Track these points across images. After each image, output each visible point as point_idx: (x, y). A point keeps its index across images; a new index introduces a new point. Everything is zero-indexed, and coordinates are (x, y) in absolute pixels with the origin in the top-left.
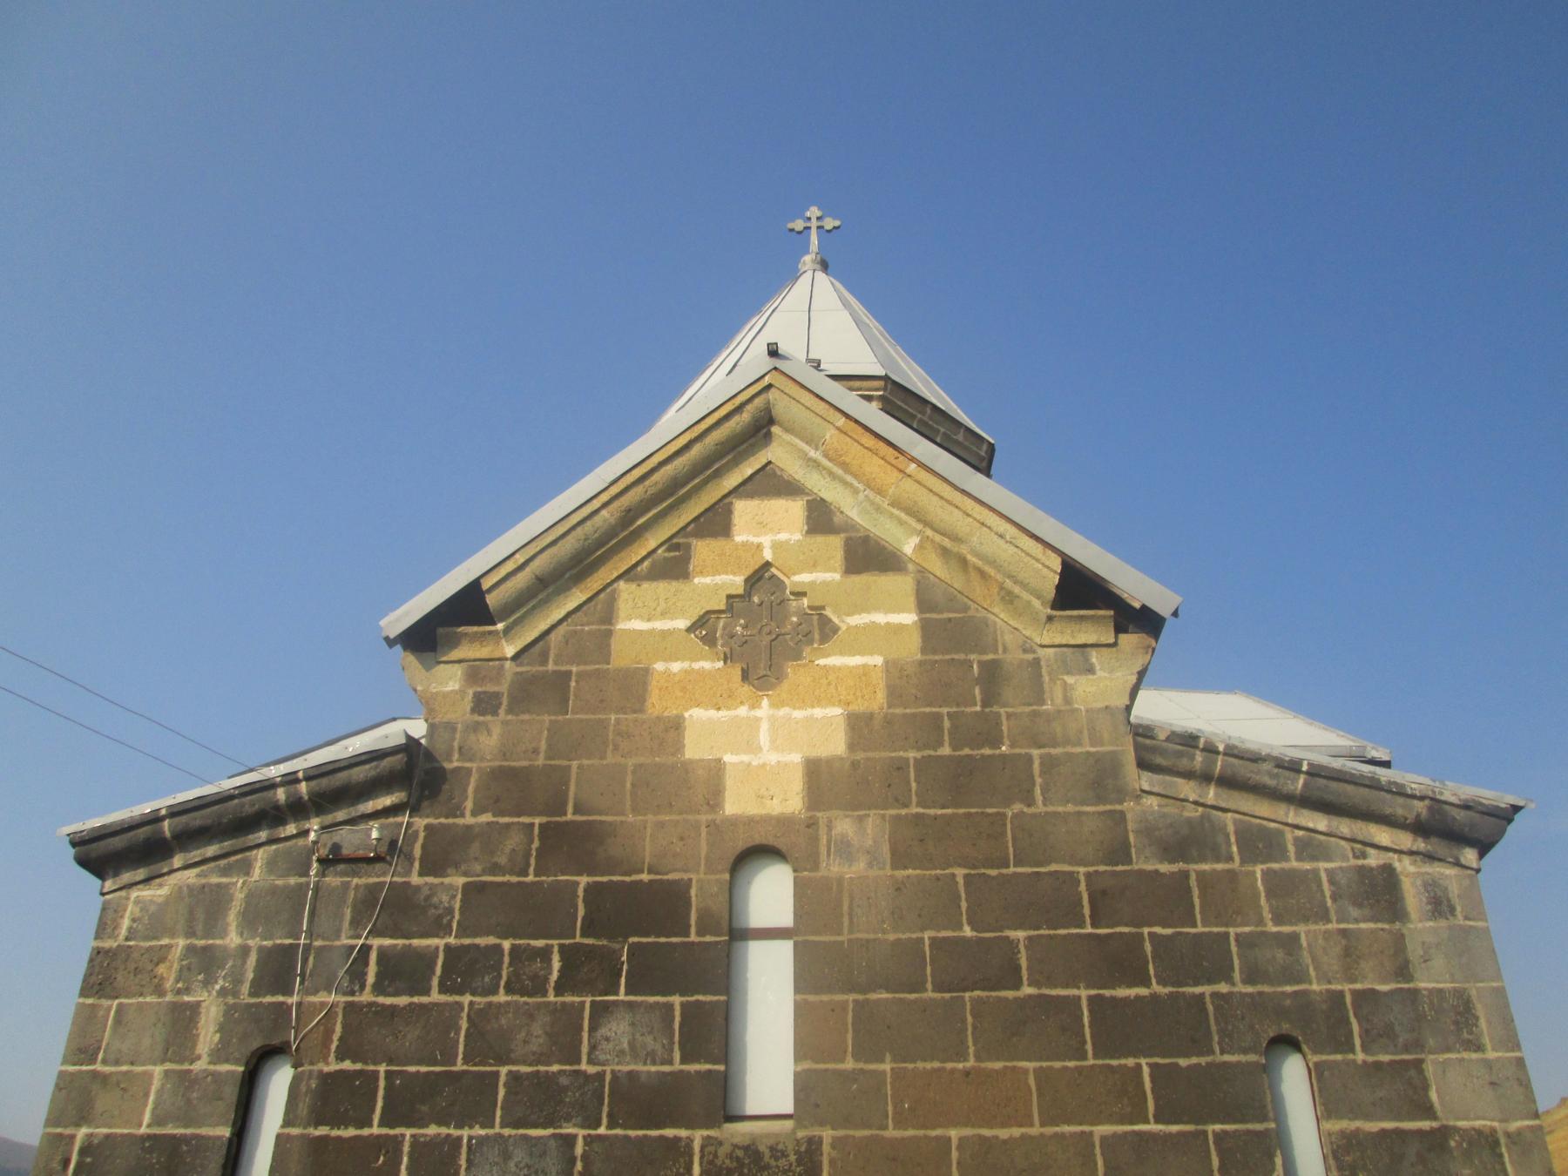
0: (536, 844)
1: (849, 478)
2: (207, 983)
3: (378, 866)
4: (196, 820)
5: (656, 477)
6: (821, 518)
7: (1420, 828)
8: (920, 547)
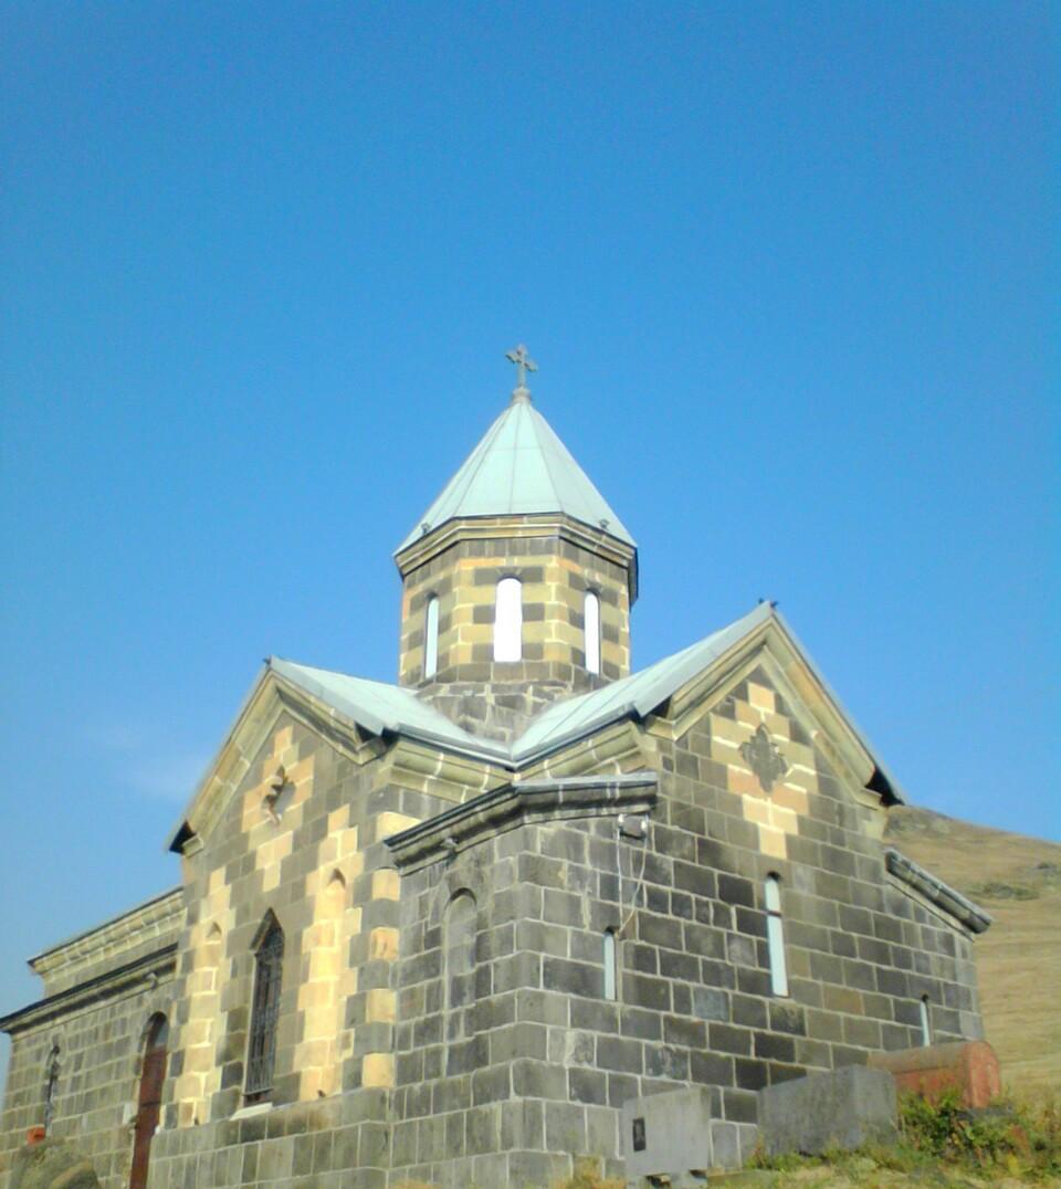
0: (697, 848)
1: (795, 690)
2: (582, 887)
3: (639, 842)
4: (575, 796)
5: (731, 661)
6: (780, 706)
7: (964, 922)
8: (817, 736)
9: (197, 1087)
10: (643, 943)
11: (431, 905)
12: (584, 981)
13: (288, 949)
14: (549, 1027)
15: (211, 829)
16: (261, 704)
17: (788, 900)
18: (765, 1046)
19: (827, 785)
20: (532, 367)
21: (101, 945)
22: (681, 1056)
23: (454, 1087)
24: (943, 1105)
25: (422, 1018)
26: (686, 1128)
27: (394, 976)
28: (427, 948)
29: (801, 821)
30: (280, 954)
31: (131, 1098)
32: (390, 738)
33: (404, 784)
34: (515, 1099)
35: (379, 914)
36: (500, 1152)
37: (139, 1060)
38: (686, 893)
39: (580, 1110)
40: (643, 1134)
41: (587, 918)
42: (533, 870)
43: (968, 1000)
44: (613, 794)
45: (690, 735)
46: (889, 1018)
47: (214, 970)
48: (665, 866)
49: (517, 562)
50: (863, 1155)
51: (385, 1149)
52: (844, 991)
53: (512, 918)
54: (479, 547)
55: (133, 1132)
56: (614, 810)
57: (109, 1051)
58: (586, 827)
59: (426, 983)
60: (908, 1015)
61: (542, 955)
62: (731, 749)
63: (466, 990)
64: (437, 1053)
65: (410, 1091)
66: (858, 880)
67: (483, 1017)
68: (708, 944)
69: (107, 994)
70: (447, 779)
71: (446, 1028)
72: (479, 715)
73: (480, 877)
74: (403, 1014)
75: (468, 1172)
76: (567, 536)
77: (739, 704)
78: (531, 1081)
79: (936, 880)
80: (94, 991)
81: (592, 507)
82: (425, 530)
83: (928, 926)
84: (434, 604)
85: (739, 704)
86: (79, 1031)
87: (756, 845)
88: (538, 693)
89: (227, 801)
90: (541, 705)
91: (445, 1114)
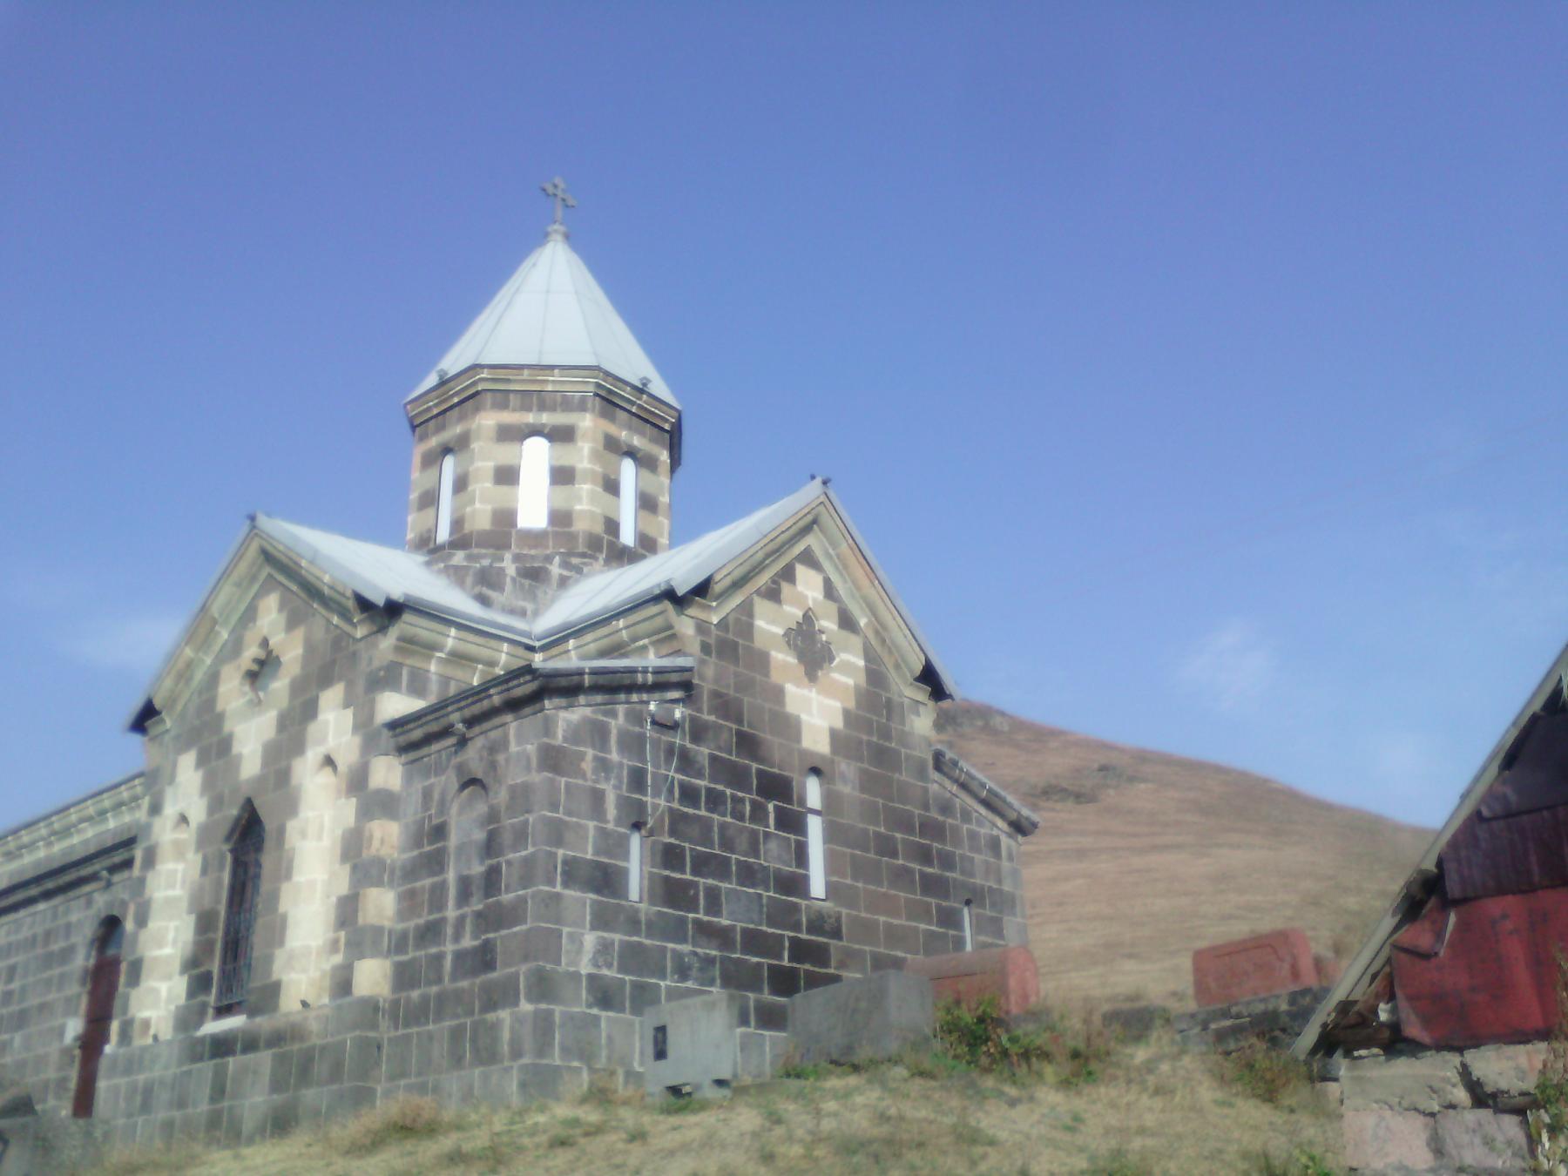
2: (607, 779)
4: (602, 680)
6: (829, 591)
8: (867, 625)
9: (158, 998)
10: (672, 840)
11: (436, 796)
12: (606, 880)
13: (269, 844)
14: (566, 930)
15: (179, 707)
16: (243, 567)
17: (830, 799)
18: (801, 951)
19: (875, 676)
20: (571, 202)
21: (43, 839)
22: (710, 961)
23: (458, 996)
24: (980, 1012)
25: (421, 921)
26: (710, 1035)
27: (392, 872)
28: (431, 843)
29: (847, 714)
30: (259, 847)
31: (75, 1014)
32: (393, 610)
33: (409, 661)
34: (526, 1007)
35: (376, 804)
36: (506, 1064)
37: (86, 971)
38: (720, 787)
39: (597, 1018)
40: (664, 1042)
41: (611, 811)
42: (553, 759)
43: (1013, 906)
44: (645, 679)
45: (731, 619)
46: (930, 923)
47: (180, 867)
48: (700, 758)
49: (546, 418)
50: (896, 1063)
51: (378, 1064)
52: (884, 894)
53: (528, 812)
54: (502, 400)
55: (77, 1052)
56: (645, 697)
57: (49, 960)
58: (614, 715)
59: (427, 882)
60: (950, 919)
61: (561, 852)
62: (774, 635)
63: (474, 889)
64: (439, 957)
65: (408, 1000)
66: (904, 777)
67: (492, 919)
68: (743, 842)
69: (47, 895)
70: (457, 658)
71: (449, 931)
72: (498, 586)
73: (493, 766)
74: (402, 915)
75: (471, 1088)
76: (603, 393)
77: (786, 588)
78: (544, 987)
79: (985, 780)
80: (34, 891)
81: (631, 362)
82: (441, 377)
83: (974, 827)
84: (449, 463)
85: (786, 588)
86: (13, 938)
87: (798, 739)
88: (565, 565)
89: (199, 676)
90: (568, 578)
91: (447, 1024)
